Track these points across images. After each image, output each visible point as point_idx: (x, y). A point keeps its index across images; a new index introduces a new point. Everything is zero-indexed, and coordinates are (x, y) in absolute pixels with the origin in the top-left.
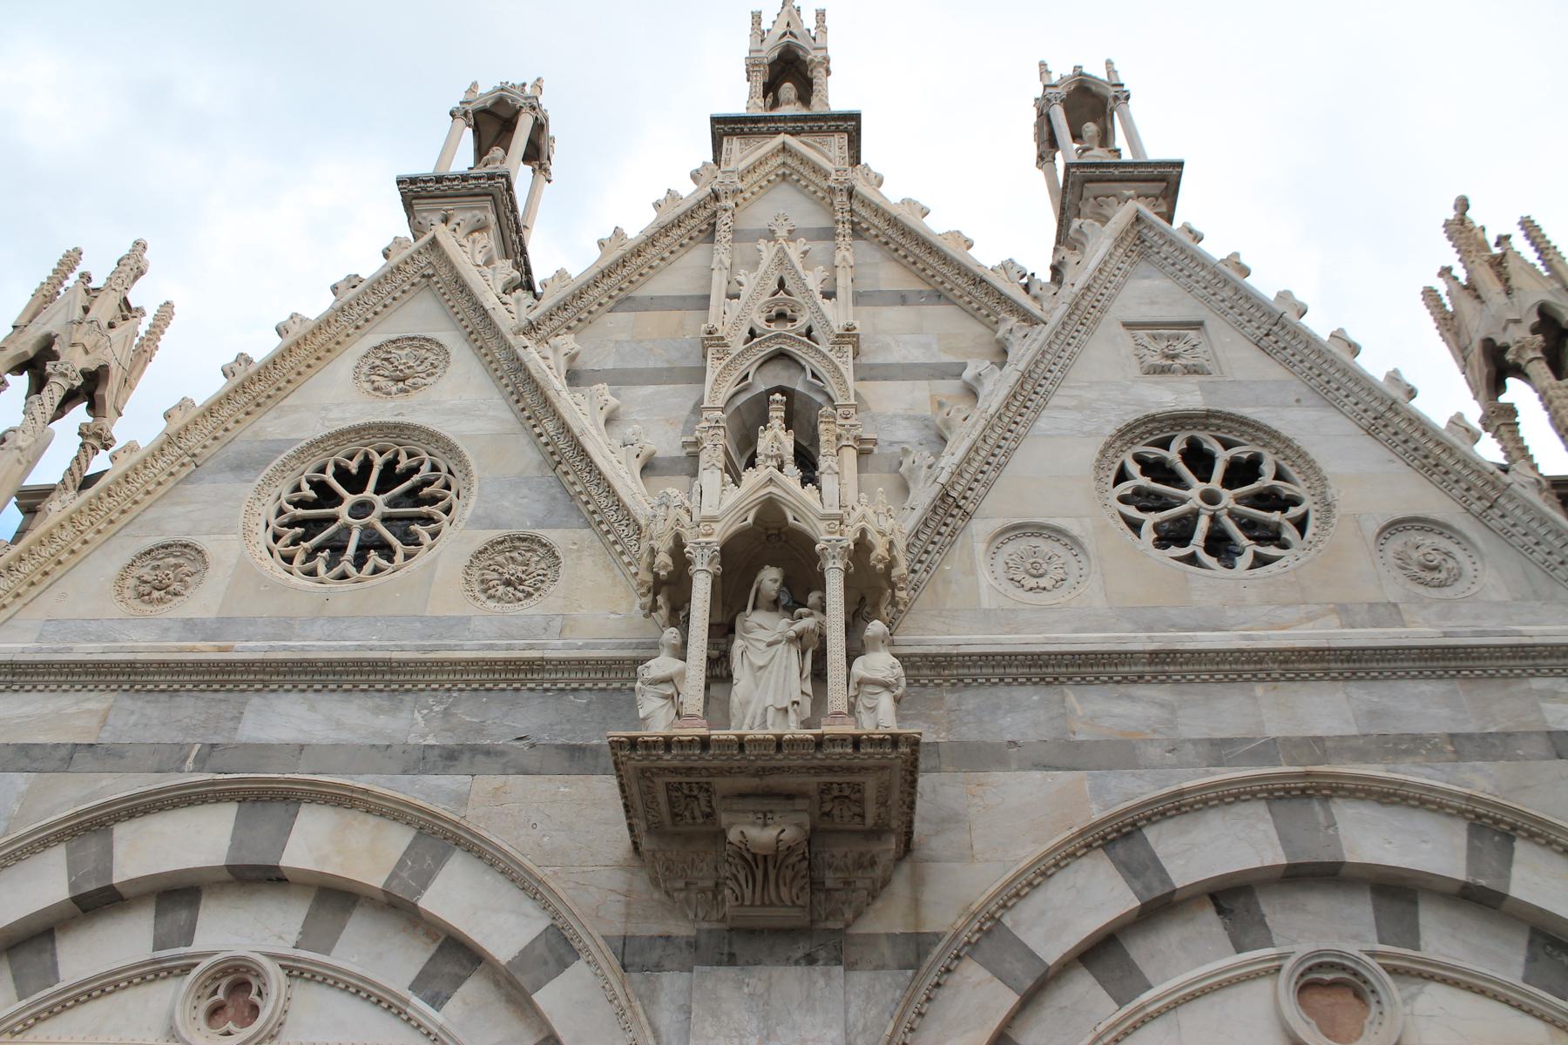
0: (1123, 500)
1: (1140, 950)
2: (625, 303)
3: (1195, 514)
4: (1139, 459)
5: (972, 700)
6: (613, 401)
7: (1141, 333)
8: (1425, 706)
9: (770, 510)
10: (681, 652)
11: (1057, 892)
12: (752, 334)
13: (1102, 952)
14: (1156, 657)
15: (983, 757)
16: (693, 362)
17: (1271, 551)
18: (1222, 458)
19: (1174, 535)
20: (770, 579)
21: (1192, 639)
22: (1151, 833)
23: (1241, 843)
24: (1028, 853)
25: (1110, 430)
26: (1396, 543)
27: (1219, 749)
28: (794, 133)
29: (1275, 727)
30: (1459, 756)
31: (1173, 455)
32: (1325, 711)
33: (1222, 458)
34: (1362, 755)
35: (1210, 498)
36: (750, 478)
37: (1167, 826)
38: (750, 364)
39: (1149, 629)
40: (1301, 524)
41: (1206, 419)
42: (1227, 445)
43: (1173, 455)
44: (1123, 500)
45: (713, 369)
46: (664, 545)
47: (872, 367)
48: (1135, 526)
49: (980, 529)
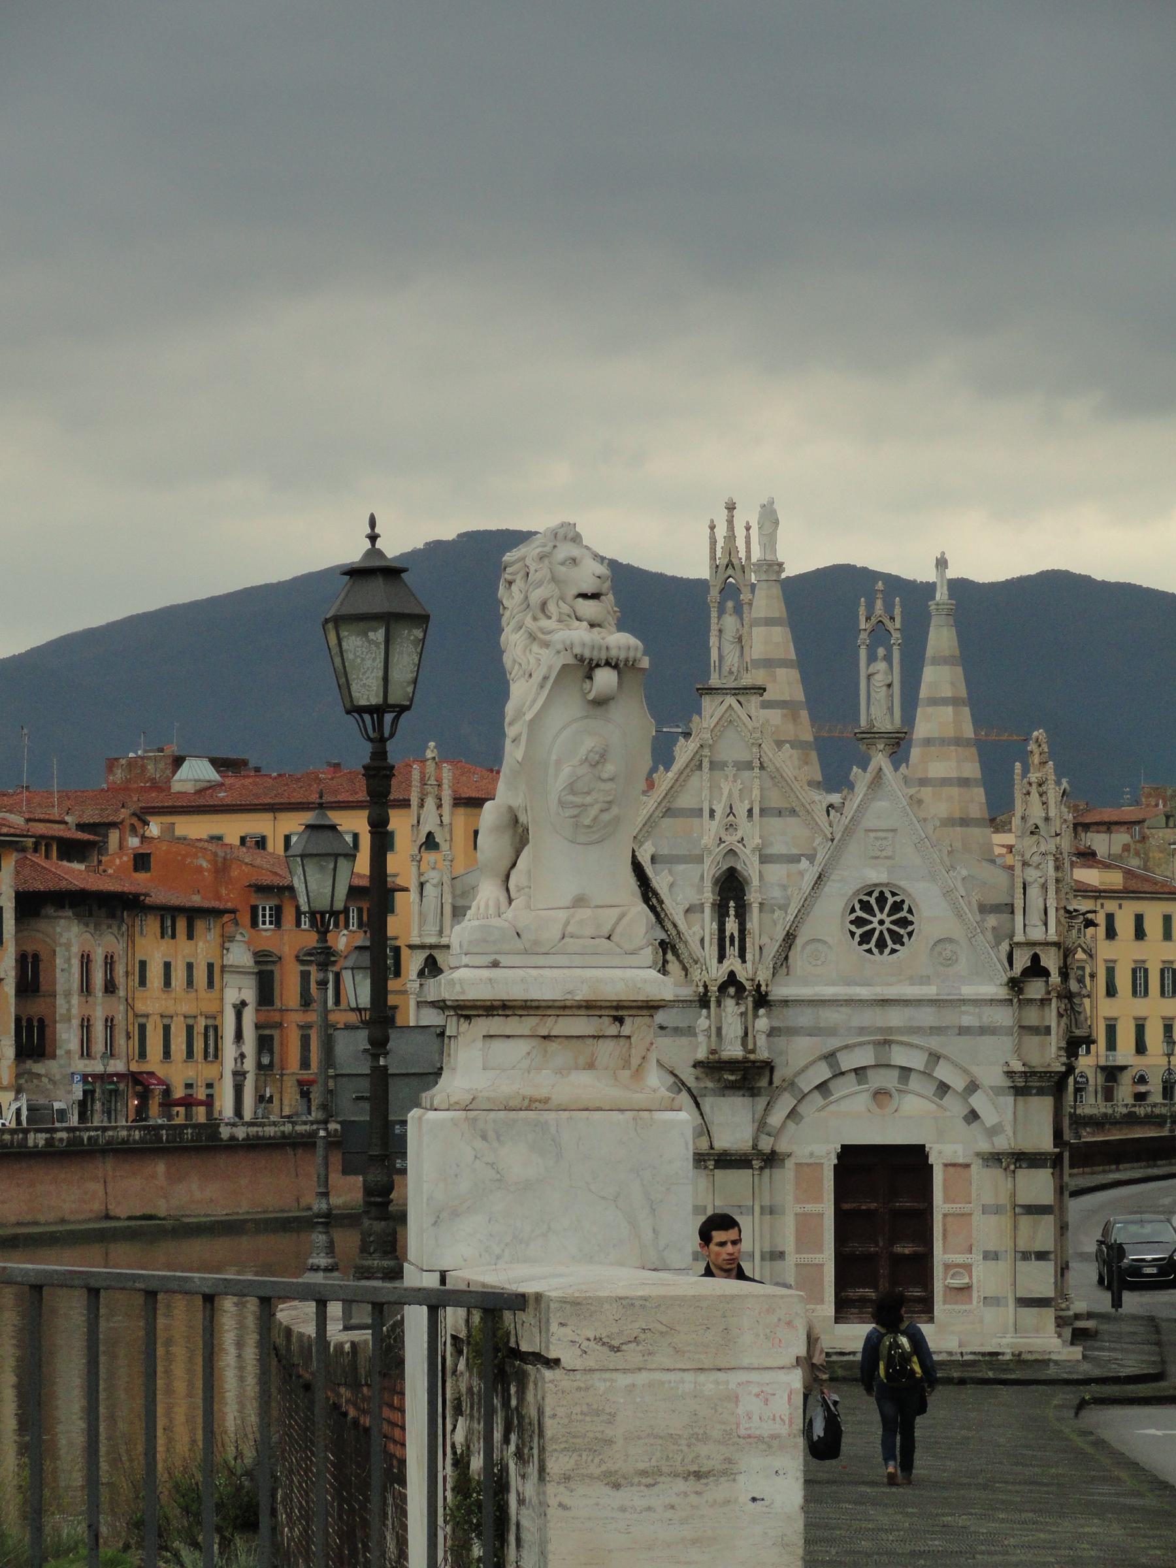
0: (852, 922)
1: (831, 1085)
2: (669, 812)
3: (874, 930)
4: (860, 901)
5: (790, 1012)
6: (671, 879)
7: (872, 835)
8: (927, 1017)
9: (732, 974)
10: (708, 1017)
11: (811, 1071)
12: (721, 841)
13: (823, 1087)
14: (846, 1001)
15: (792, 1031)
16: (697, 852)
17: (897, 947)
18: (891, 900)
19: (865, 938)
20: (732, 990)
21: (859, 995)
22: (838, 1055)
23: (864, 1057)
24: (803, 1063)
25: (850, 893)
26: (938, 949)
27: (862, 1030)
28: (735, 694)
29: (879, 1024)
30: (931, 1034)
31: (873, 901)
32: (895, 1018)
33: (891, 900)
34: (902, 1034)
35: (881, 922)
36: (726, 963)
37: (844, 1051)
38: (720, 857)
39: (848, 985)
40: (910, 934)
41: (887, 885)
42: (894, 894)
43: (873, 901)
44: (852, 922)
45: (707, 861)
46: (701, 984)
47: (766, 856)
48: (853, 934)
49: (799, 942)
